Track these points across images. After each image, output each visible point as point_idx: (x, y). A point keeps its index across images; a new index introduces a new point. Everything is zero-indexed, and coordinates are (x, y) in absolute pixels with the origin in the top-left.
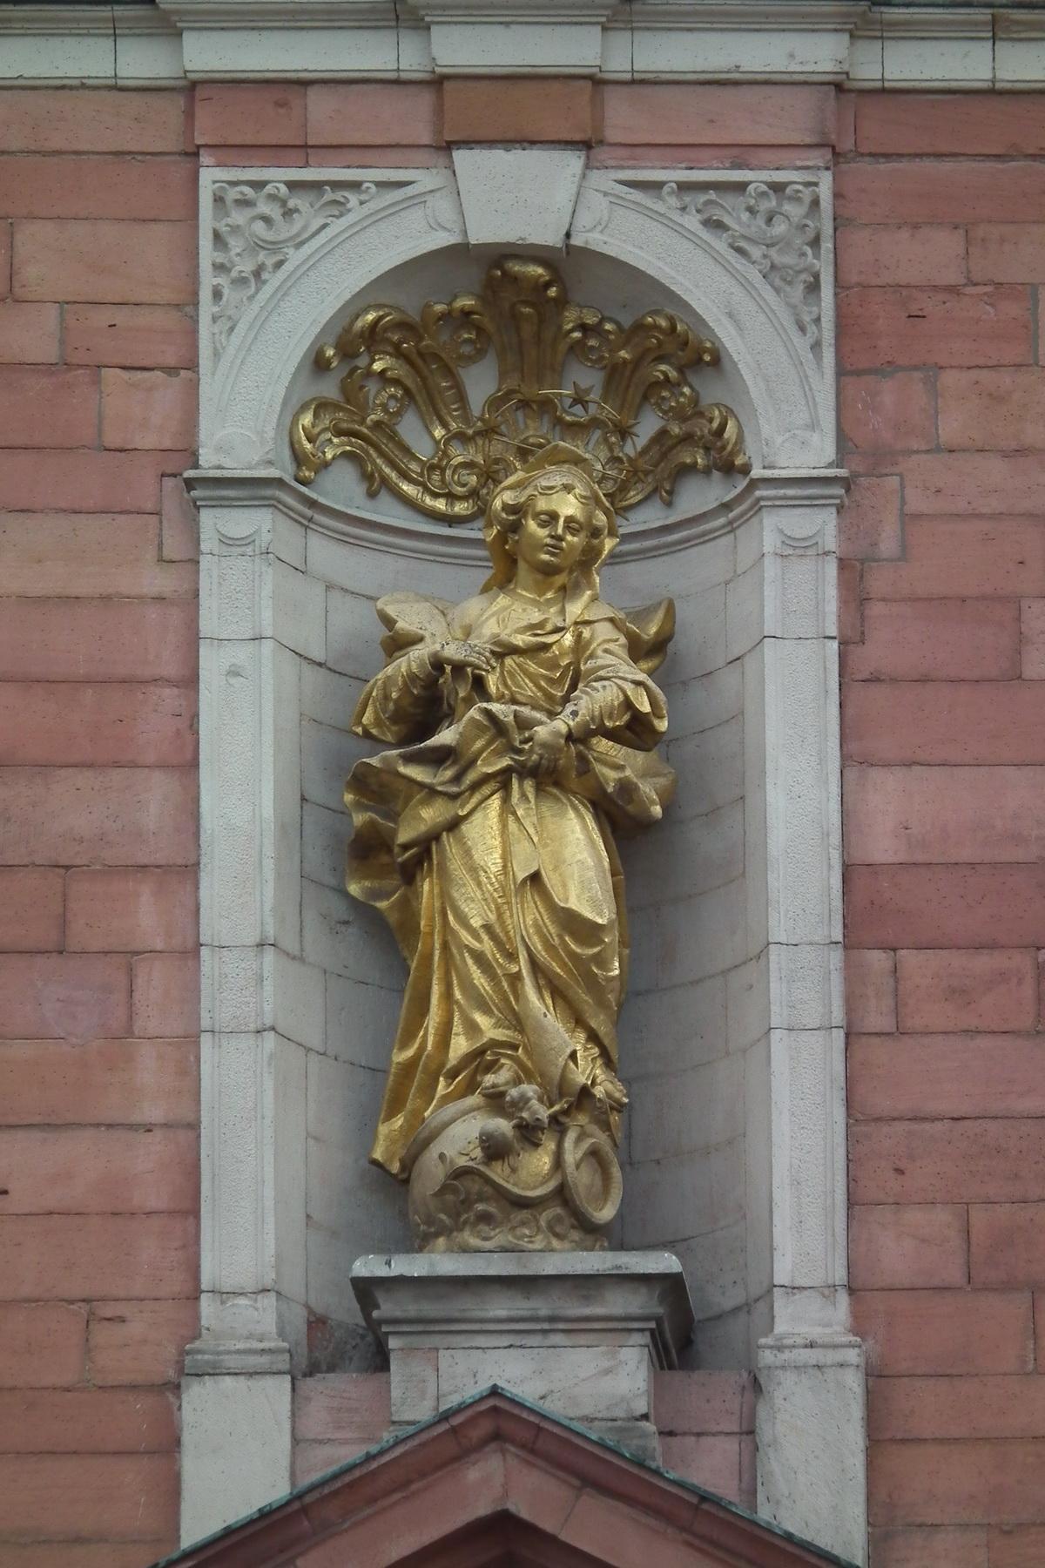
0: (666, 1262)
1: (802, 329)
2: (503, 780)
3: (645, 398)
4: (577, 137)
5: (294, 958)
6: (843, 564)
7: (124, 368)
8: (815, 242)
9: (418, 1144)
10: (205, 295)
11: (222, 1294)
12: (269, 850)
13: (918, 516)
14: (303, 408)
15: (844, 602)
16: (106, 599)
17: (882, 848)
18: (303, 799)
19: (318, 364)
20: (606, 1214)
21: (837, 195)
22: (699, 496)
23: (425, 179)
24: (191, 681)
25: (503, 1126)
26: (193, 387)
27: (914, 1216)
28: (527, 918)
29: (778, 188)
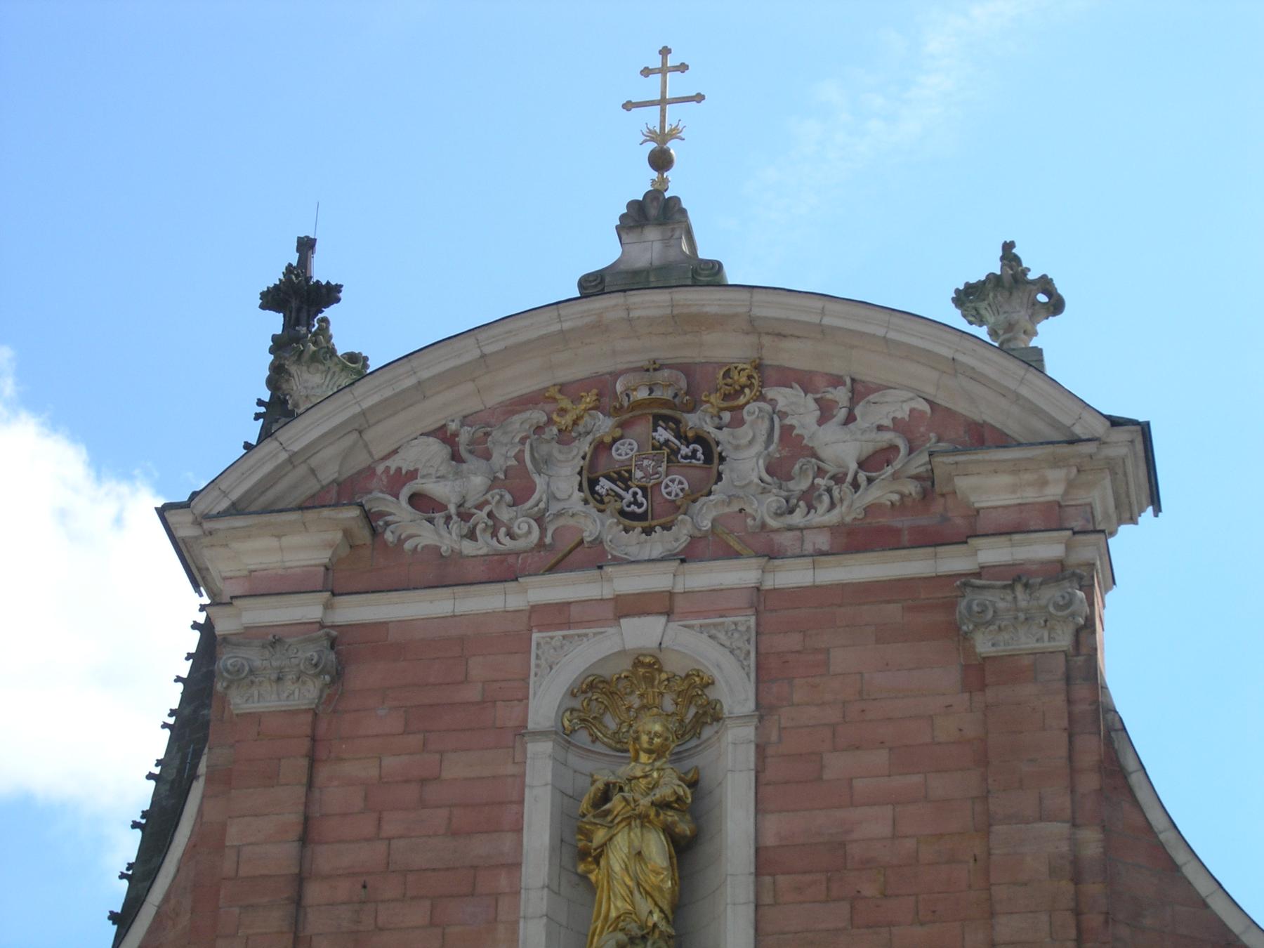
1: (744, 669)
2: (628, 820)
3: (691, 703)
4: (664, 611)
5: (556, 893)
6: (757, 746)
7: (503, 701)
8: (748, 641)
10: (532, 674)
12: (547, 854)
13: (785, 728)
14: (566, 710)
16: (494, 777)
17: (770, 840)
18: (562, 841)
21: (758, 624)
23: (611, 630)
24: (521, 802)
26: (527, 706)
29: (736, 624)
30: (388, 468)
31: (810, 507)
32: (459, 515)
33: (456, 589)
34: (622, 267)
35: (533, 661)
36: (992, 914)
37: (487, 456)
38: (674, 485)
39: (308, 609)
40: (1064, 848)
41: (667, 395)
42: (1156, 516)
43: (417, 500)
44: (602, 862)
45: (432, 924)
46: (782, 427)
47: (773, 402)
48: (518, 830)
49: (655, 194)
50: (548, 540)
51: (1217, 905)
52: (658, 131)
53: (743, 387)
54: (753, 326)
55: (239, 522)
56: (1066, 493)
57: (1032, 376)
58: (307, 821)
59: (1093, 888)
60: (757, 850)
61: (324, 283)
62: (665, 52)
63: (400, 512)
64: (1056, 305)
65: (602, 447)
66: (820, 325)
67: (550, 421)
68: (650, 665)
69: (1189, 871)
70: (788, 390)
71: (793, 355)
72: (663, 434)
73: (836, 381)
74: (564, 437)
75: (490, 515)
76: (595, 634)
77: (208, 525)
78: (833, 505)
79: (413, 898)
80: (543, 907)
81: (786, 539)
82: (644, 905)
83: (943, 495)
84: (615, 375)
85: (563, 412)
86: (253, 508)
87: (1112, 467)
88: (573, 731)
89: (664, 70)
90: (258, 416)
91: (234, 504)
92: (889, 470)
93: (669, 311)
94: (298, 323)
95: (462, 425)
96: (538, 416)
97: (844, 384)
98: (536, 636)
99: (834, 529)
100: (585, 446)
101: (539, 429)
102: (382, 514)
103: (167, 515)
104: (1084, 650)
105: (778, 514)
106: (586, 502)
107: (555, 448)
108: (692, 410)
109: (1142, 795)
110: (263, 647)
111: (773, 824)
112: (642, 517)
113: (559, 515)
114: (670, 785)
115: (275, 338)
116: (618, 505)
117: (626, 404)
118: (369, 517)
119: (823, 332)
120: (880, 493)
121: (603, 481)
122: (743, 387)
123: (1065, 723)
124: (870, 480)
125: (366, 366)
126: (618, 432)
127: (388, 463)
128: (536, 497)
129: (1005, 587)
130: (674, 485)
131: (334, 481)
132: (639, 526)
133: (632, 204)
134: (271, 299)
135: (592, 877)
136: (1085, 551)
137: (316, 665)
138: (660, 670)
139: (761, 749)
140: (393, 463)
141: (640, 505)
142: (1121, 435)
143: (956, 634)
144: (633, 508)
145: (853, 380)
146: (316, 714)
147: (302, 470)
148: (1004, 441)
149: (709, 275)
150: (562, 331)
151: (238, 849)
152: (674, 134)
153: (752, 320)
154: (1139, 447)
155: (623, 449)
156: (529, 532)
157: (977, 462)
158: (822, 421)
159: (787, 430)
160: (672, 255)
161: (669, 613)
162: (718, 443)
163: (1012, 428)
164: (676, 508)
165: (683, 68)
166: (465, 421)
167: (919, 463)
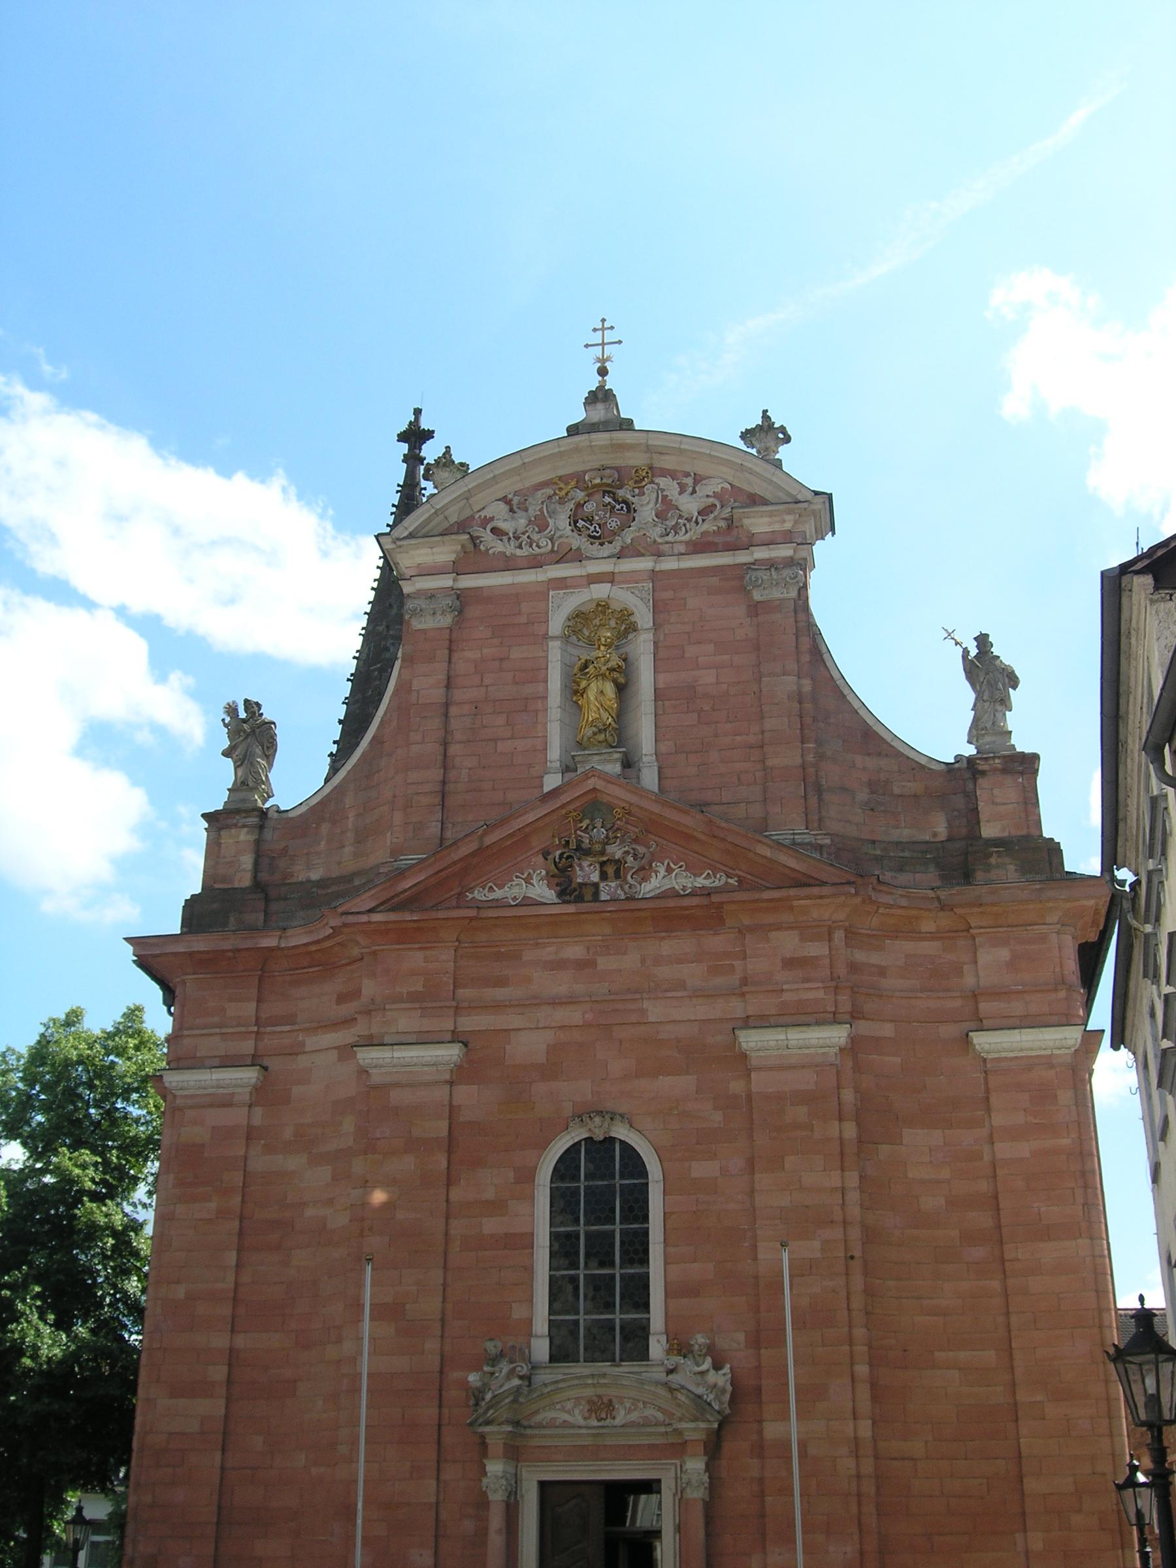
0: (624, 749)
11: (551, 762)
12: (559, 692)
15: (654, 649)
17: (661, 685)
20: (615, 744)
25: (596, 730)
27: (666, 742)
30: (480, 516)
31: (676, 533)
32: (514, 537)
33: (514, 572)
34: (586, 422)
35: (550, 604)
36: (762, 718)
37: (526, 510)
38: (613, 523)
39: (446, 581)
40: (795, 688)
41: (610, 481)
42: (833, 536)
43: (495, 531)
44: (585, 696)
45: (508, 724)
46: (662, 496)
47: (658, 484)
49: (601, 387)
50: (556, 549)
51: (862, 712)
52: (601, 357)
53: (644, 478)
54: (648, 449)
55: (413, 541)
56: (793, 526)
57: (778, 471)
58: (449, 678)
59: (808, 706)
60: (655, 690)
61: (426, 429)
62: (603, 320)
63: (487, 536)
64: (787, 439)
65: (579, 506)
66: (680, 448)
67: (555, 494)
68: (605, 606)
69: (850, 698)
70: (664, 479)
71: (667, 462)
72: (608, 499)
73: (687, 475)
74: (562, 501)
76: (579, 592)
77: (399, 543)
78: (686, 532)
79: (500, 713)
80: (558, 716)
81: (666, 548)
82: (605, 715)
83: (737, 527)
84: (585, 472)
85: (561, 489)
86: (419, 535)
87: (814, 513)
88: (569, 636)
89: (603, 329)
90: (397, 492)
91: (410, 534)
92: (712, 516)
93: (609, 442)
94: (415, 448)
95: (514, 495)
96: (549, 491)
97: (691, 476)
98: (551, 593)
99: (687, 543)
100: (572, 505)
101: (550, 497)
102: (478, 537)
103: (379, 539)
104: (802, 598)
106: (573, 531)
107: (558, 506)
108: (621, 488)
110: (426, 599)
111: (662, 677)
112: (599, 538)
113: (560, 537)
114: (615, 661)
115: (404, 455)
116: (587, 532)
117: (590, 485)
118: (473, 539)
119: (681, 451)
120: (708, 526)
121: (580, 521)
122: (644, 478)
123: (795, 631)
124: (703, 520)
125: (468, 469)
126: (587, 498)
127: (480, 513)
128: (549, 528)
129: (766, 569)
130: (613, 523)
131: (456, 522)
132: (597, 542)
133: (590, 392)
134: (402, 438)
135: (580, 702)
136: (802, 553)
137: (451, 607)
138: (609, 608)
140: (483, 514)
141: (598, 532)
142: (819, 499)
143: (744, 591)
144: (595, 533)
145: (695, 474)
146: (451, 630)
147: (441, 517)
148: (765, 502)
149: (627, 425)
150: (560, 452)
151: (418, 691)
152: (609, 359)
153: (648, 446)
154: (827, 505)
156: (547, 545)
157: (754, 512)
158: (681, 493)
159: (665, 497)
160: (609, 416)
161: (612, 582)
162: (633, 504)
163: (768, 496)
164: (614, 533)
165: (612, 328)
166: (516, 493)
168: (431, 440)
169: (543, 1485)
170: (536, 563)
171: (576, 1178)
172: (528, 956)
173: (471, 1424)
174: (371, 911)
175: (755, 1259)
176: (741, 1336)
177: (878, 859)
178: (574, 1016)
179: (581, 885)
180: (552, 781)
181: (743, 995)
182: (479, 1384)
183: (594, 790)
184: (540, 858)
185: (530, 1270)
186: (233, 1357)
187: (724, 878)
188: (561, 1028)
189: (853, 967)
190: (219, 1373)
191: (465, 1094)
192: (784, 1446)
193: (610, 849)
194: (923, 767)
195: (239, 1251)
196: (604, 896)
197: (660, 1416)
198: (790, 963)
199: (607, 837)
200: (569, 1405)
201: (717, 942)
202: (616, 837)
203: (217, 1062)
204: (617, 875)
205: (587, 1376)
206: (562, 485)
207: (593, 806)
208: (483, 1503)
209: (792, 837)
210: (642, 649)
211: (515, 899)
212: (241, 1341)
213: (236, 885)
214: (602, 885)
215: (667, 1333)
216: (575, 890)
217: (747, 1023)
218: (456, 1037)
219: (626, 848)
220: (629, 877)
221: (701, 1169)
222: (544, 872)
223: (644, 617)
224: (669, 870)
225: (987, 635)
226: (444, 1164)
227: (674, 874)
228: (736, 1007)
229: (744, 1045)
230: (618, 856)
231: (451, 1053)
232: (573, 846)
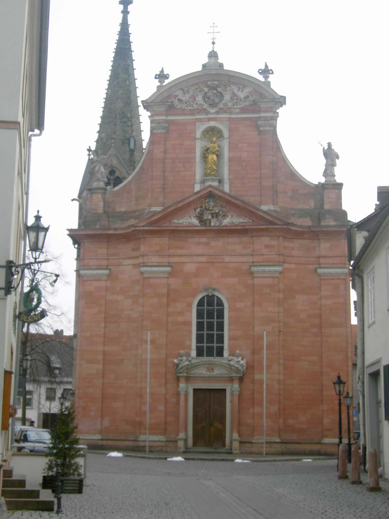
0: (219, 178)
9: (207, 172)
19: (202, 132)
22: (222, 139)
25: (211, 171)
28: (212, 160)
37: (189, 93)
44: (207, 159)
48: (195, 153)
49: (213, 50)
51: (291, 167)
63: (176, 102)
64: (273, 73)
65: (206, 93)
69: (288, 162)
75: (190, 103)
81: (233, 110)
89: (214, 27)
92: (248, 100)
96: (196, 87)
99: (240, 108)
100: (203, 93)
101: (196, 89)
105: (231, 106)
106: (203, 102)
109: (282, 151)
112: (212, 105)
114: (217, 148)
116: (209, 103)
120: (247, 104)
128: (196, 101)
130: (217, 100)
132: (211, 106)
139: (230, 143)
140: (175, 93)
144: (211, 103)
149: (221, 65)
152: (215, 38)
155: (209, 94)
156: (195, 106)
158: (238, 91)
159: (233, 92)
161: (216, 121)
167: (252, 99)
168: (132, 4)
169: (195, 390)
170: (192, 112)
171: (204, 306)
172: (190, 240)
173: (176, 373)
174: (143, 226)
175: (254, 331)
176: (249, 351)
177: (293, 215)
178: (203, 259)
179: (206, 220)
180: (197, 188)
181: (253, 255)
182: (178, 363)
183: (210, 191)
184: (193, 211)
185: (190, 332)
186: (104, 353)
187: (248, 220)
188: (200, 262)
189: (285, 248)
190: (101, 357)
191: (172, 281)
192: (261, 382)
193: (215, 209)
194: (308, 185)
195: (105, 322)
196: (212, 224)
197: (226, 372)
198: (267, 246)
199: (214, 205)
200: (202, 368)
201: (245, 239)
202: (216, 205)
203: (95, 267)
204: (217, 217)
205: (207, 361)
206: (200, 85)
207: (210, 195)
208: (178, 394)
209: (268, 208)
210: (225, 144)
211: (186, 223)
212: (107, 348)
213: (98, 212)
214: (212, 220)
215: (229, 350)
216: (204, 221)
217: (253, 264)
218: (169, 265)
219: (220, 209)
220: (220, 219)
221: (239, 305)
222: (195, 215)
223: (226, 134)
224: (232, 216)
225: (331, 143)
226: (166, 301)
227: (233, 218)
228: (250, 259)
229: (252, 271)
230: (217, 211)
231: (168, 269)
232: (204, 208)
